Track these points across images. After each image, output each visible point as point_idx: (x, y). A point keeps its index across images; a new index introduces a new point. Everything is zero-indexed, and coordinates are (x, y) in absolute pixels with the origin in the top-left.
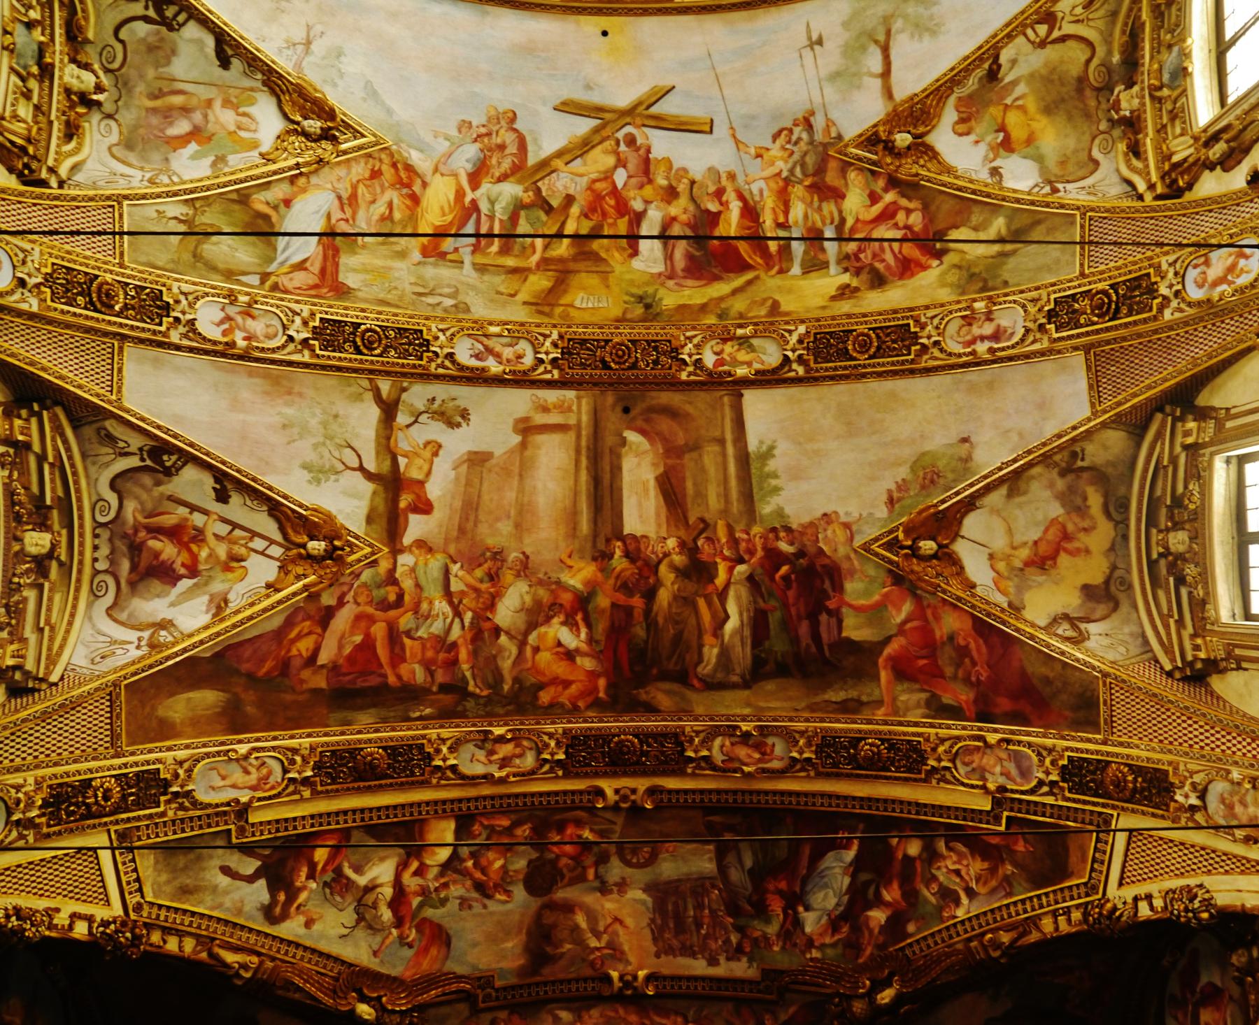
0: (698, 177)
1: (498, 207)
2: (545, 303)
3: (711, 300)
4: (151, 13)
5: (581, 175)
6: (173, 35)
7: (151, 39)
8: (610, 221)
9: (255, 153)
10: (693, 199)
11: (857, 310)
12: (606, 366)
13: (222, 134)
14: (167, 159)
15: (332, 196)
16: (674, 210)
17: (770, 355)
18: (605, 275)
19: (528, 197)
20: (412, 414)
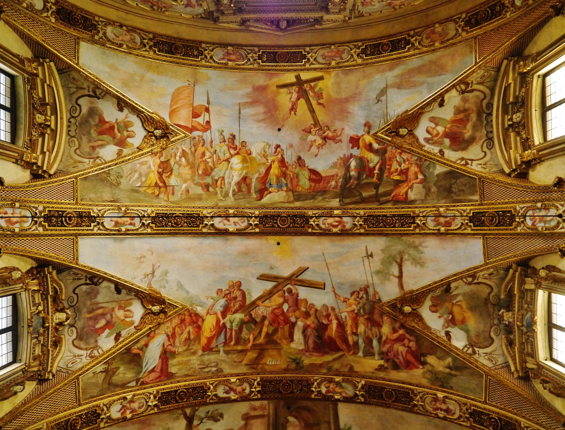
0: (319, 308)
1: (234, 325)
2: (254, 364)
3: (324, 362)
4: (88, 282)
5: (269, 307)
6: (98, 287)
7: (88, 291)
8: (281, 326)
9: (133, 327)
10: (316, 317)
11: (387, 377)
12: (280, 392)
13: (119, 321)
14: (96, 341)
15: (165, 336)
16: (308, 322)
17: (350, 391)
18: (279, 350)
19: (247, 319)
20: (199, 419)
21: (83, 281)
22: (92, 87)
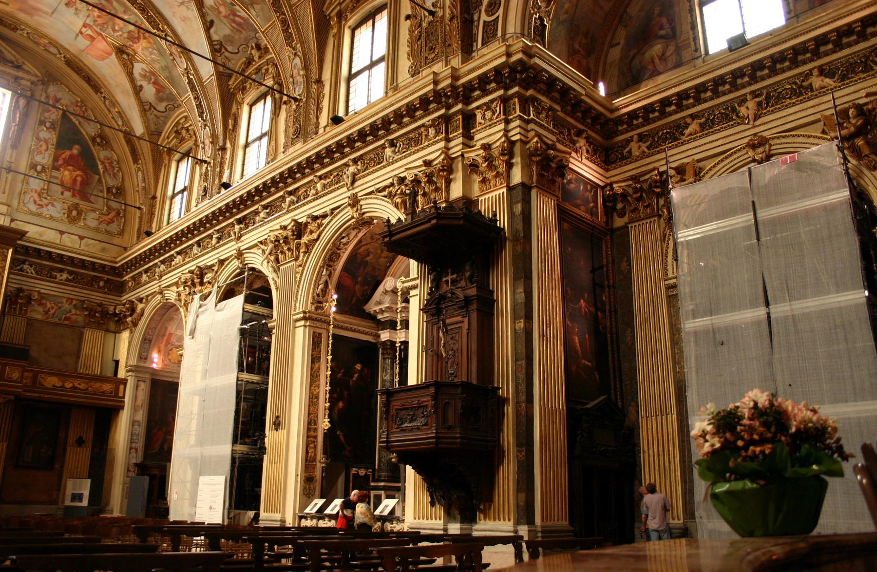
4: (223, 50)
21: (226, 54)
22: (148, 113)
